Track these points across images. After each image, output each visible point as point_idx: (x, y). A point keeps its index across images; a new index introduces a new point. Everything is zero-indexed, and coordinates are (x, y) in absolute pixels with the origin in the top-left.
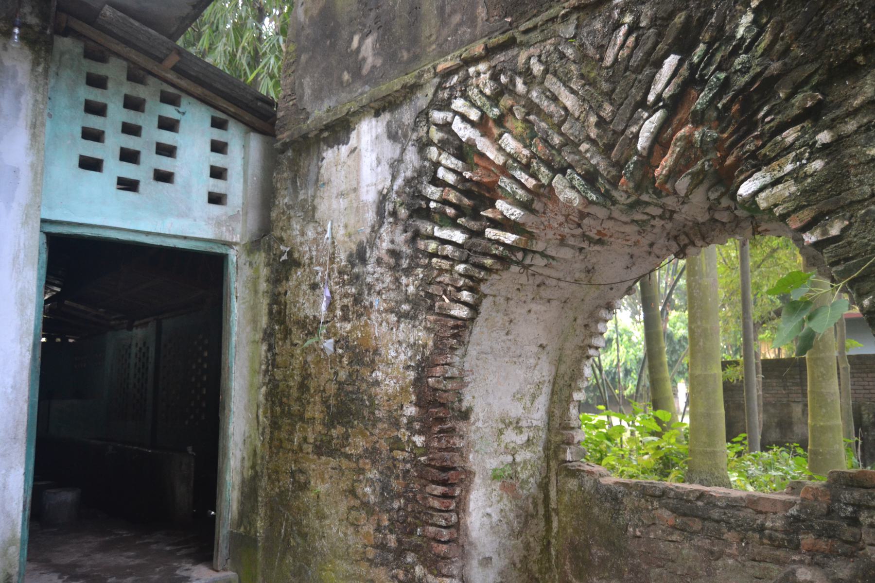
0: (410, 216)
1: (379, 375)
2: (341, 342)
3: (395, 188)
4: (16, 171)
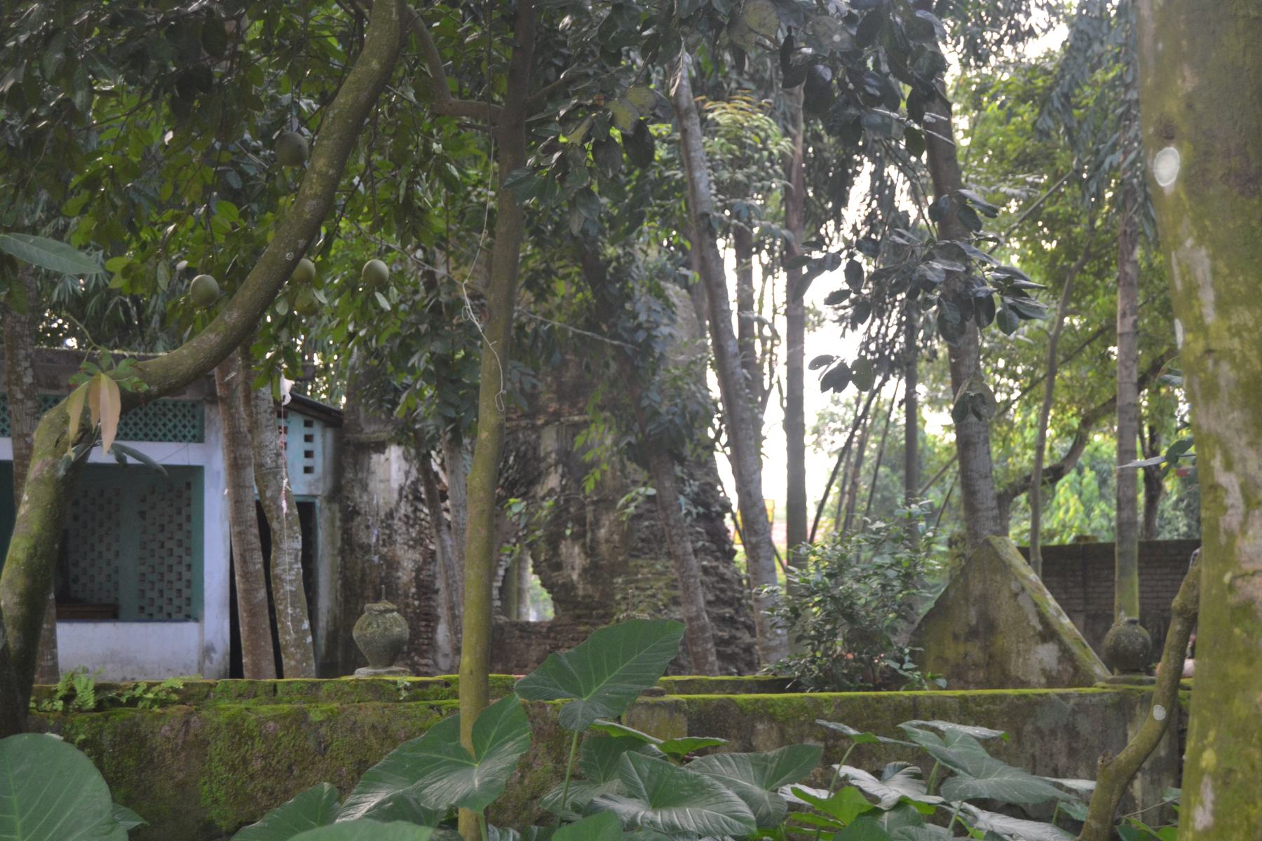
1: (400, 574)
2: (382, 557)
4: (218, 473)
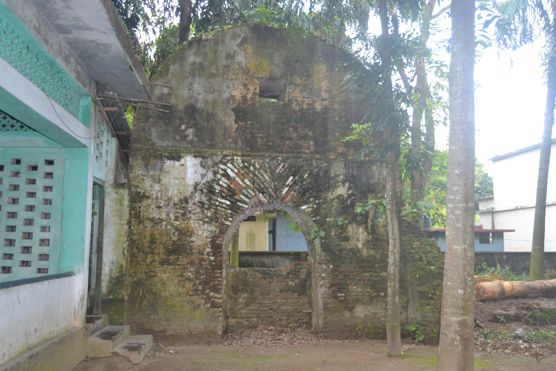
0: (208, 193)
1: (193, 239)
3: (202, 182)
